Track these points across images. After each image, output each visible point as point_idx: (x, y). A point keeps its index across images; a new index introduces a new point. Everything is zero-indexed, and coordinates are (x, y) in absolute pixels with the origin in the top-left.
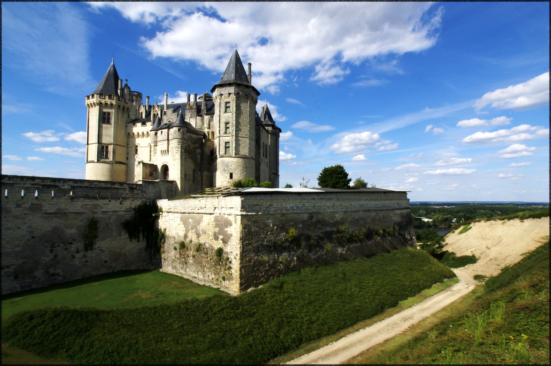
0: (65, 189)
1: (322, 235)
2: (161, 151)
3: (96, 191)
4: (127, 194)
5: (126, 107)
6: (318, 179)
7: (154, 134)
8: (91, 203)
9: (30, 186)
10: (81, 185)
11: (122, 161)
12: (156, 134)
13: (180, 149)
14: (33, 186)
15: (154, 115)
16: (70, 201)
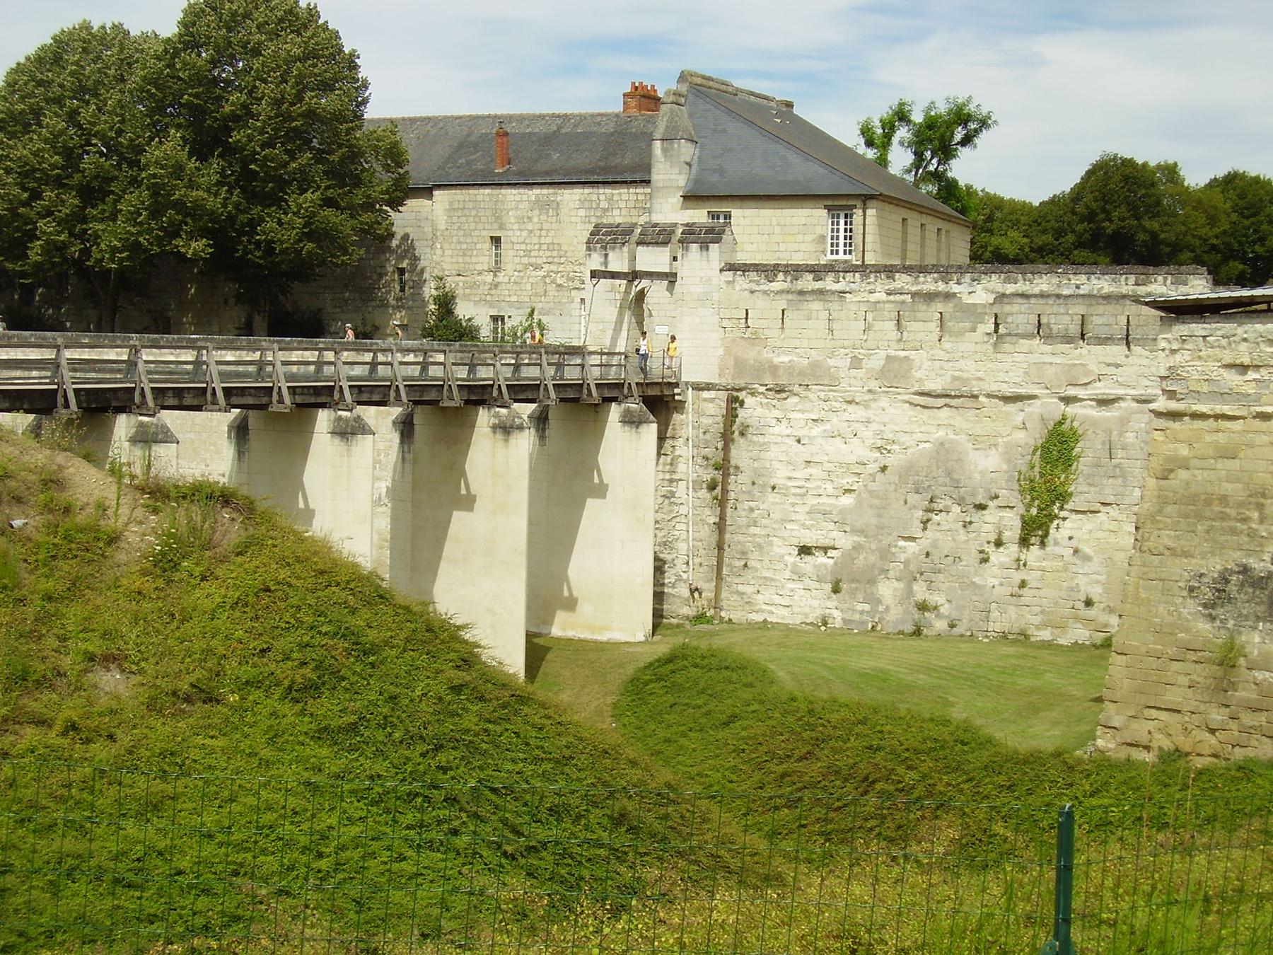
0: (974, 305)
3: (1078, 309)
8: (1057, 360)
9: (883, 296)
14: (892, 298)
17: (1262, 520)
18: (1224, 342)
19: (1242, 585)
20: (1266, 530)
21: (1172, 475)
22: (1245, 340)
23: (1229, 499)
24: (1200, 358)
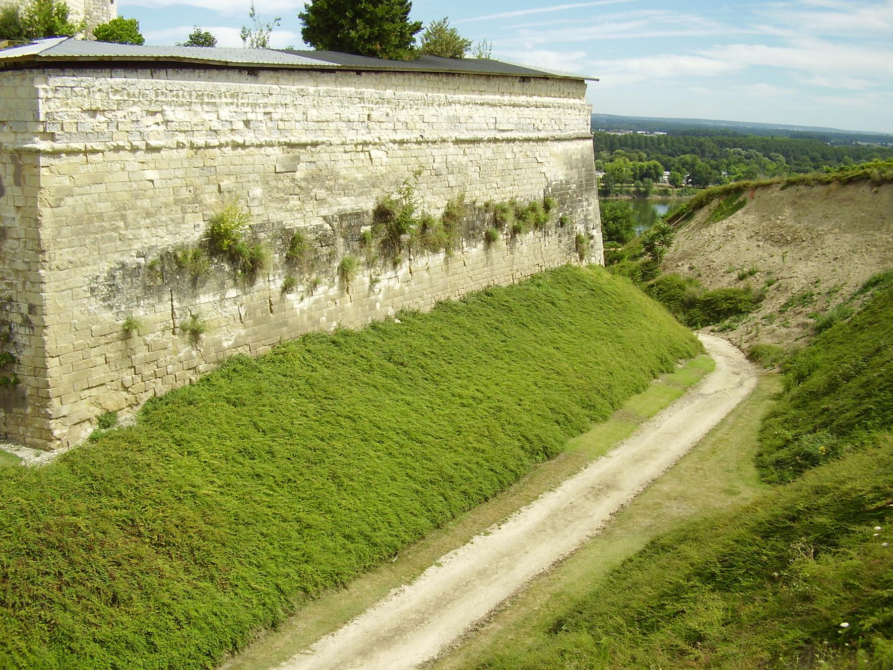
1: (327, 226)
6: (301, 16)
17: (126, 228)
18: (85, 92)
19: (124, 278)
20: (131, 233)
21: (62, 203)
22: (100, 90)
23: (105, 215)
24: (67, 104)
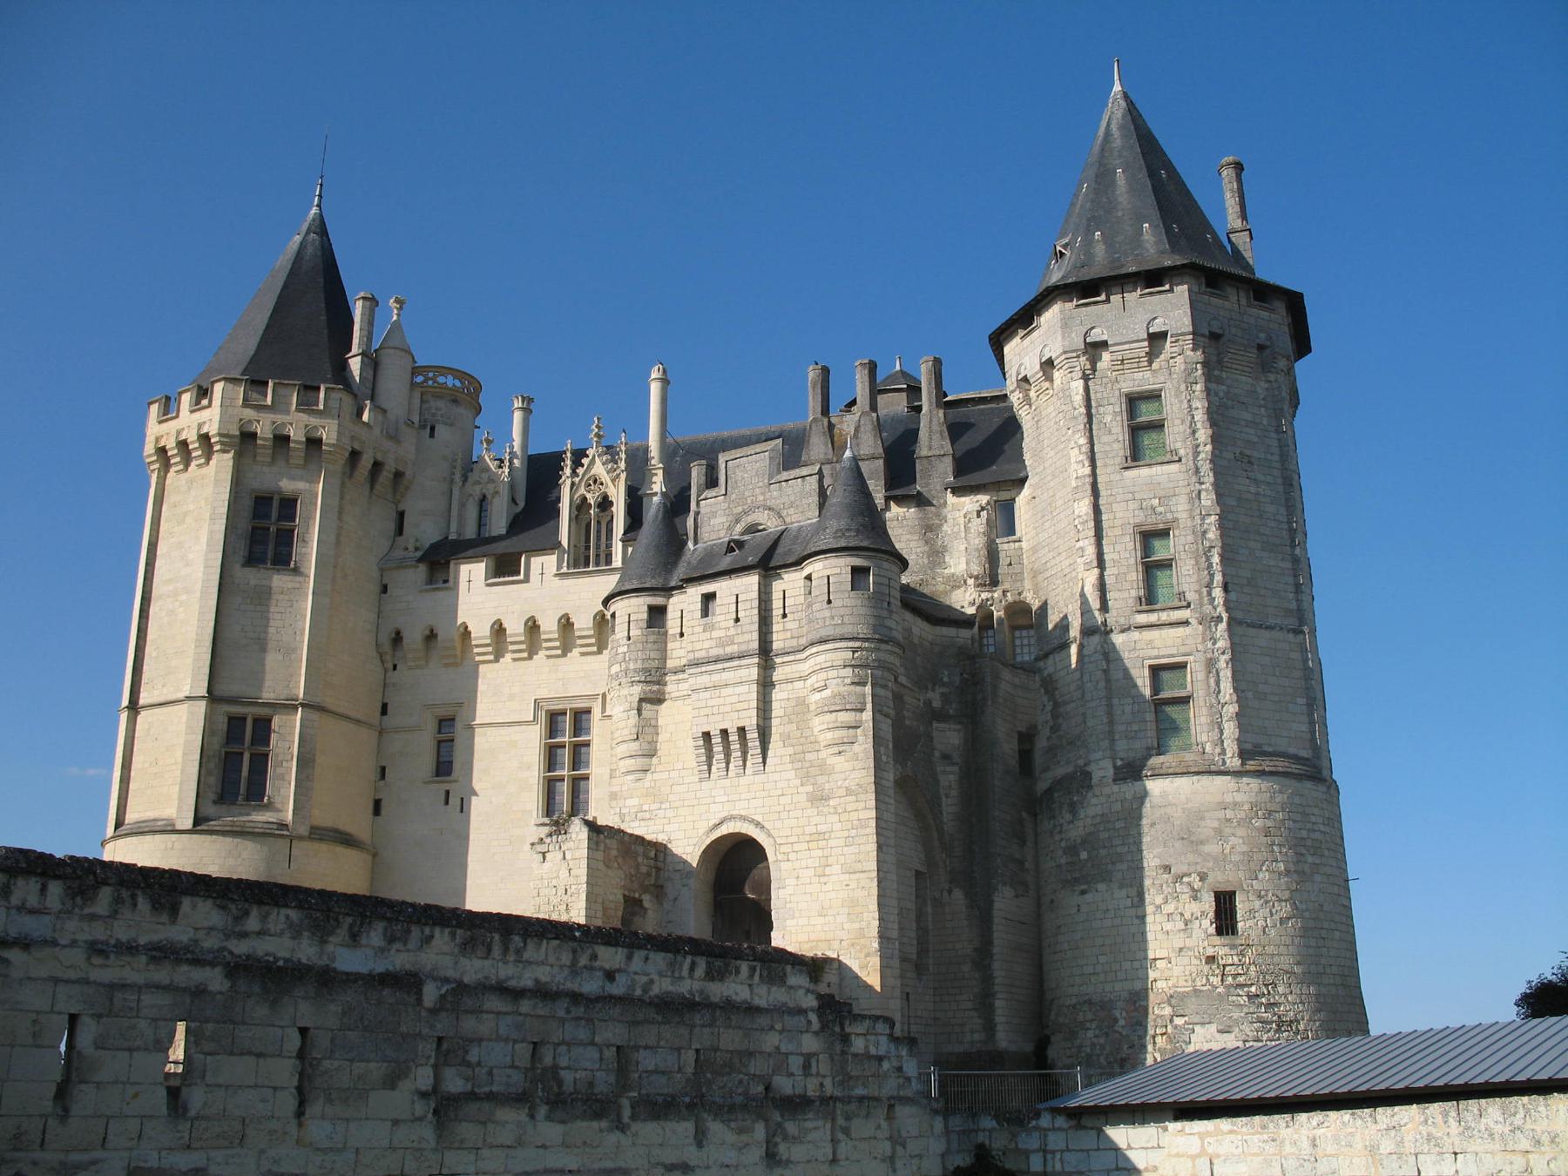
2: (707, 736)
3: (612, 1032)
4: (806, 1067)
5: (390, 467)
7: (645, 616)
10: (506, 971)
11: (346, 825)
12: (657, 615)
13: (867, 715)
14: (162, 974)
15: (581, 507)
16: (427, 1132)
